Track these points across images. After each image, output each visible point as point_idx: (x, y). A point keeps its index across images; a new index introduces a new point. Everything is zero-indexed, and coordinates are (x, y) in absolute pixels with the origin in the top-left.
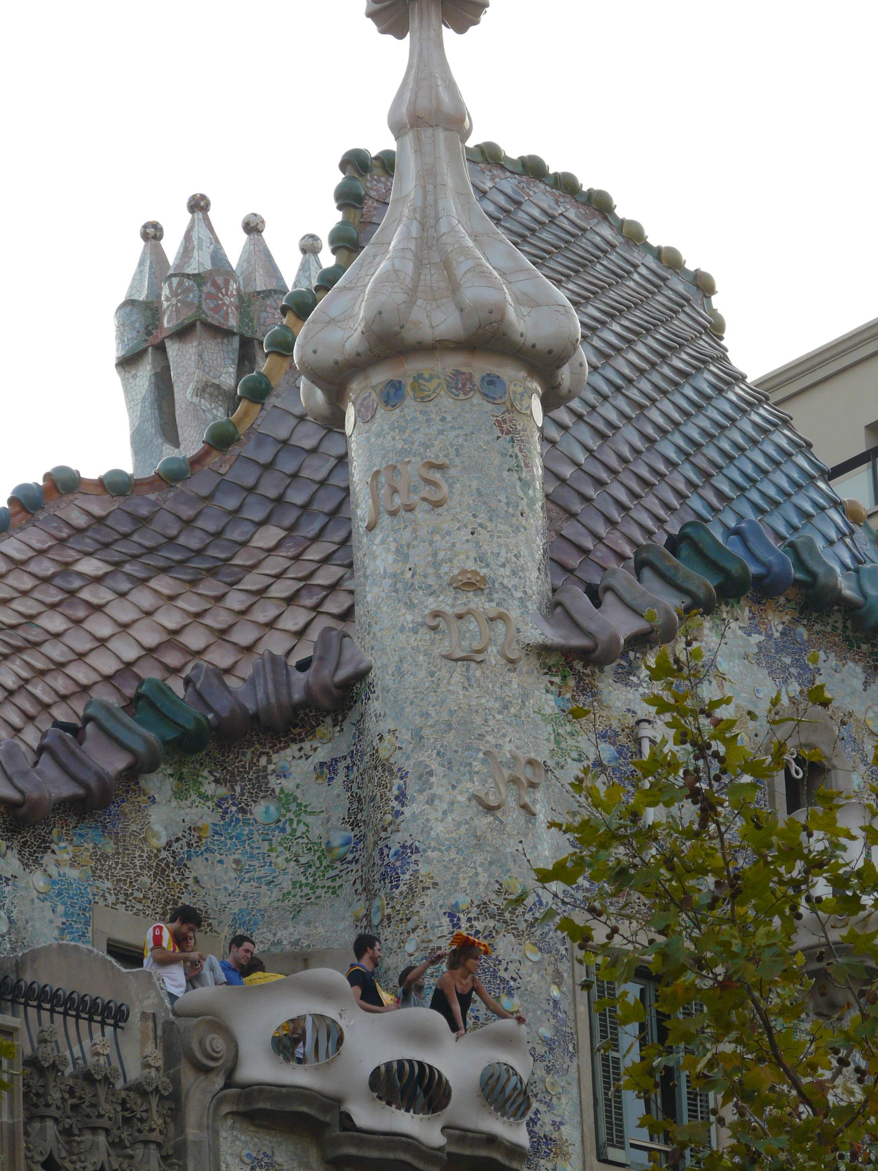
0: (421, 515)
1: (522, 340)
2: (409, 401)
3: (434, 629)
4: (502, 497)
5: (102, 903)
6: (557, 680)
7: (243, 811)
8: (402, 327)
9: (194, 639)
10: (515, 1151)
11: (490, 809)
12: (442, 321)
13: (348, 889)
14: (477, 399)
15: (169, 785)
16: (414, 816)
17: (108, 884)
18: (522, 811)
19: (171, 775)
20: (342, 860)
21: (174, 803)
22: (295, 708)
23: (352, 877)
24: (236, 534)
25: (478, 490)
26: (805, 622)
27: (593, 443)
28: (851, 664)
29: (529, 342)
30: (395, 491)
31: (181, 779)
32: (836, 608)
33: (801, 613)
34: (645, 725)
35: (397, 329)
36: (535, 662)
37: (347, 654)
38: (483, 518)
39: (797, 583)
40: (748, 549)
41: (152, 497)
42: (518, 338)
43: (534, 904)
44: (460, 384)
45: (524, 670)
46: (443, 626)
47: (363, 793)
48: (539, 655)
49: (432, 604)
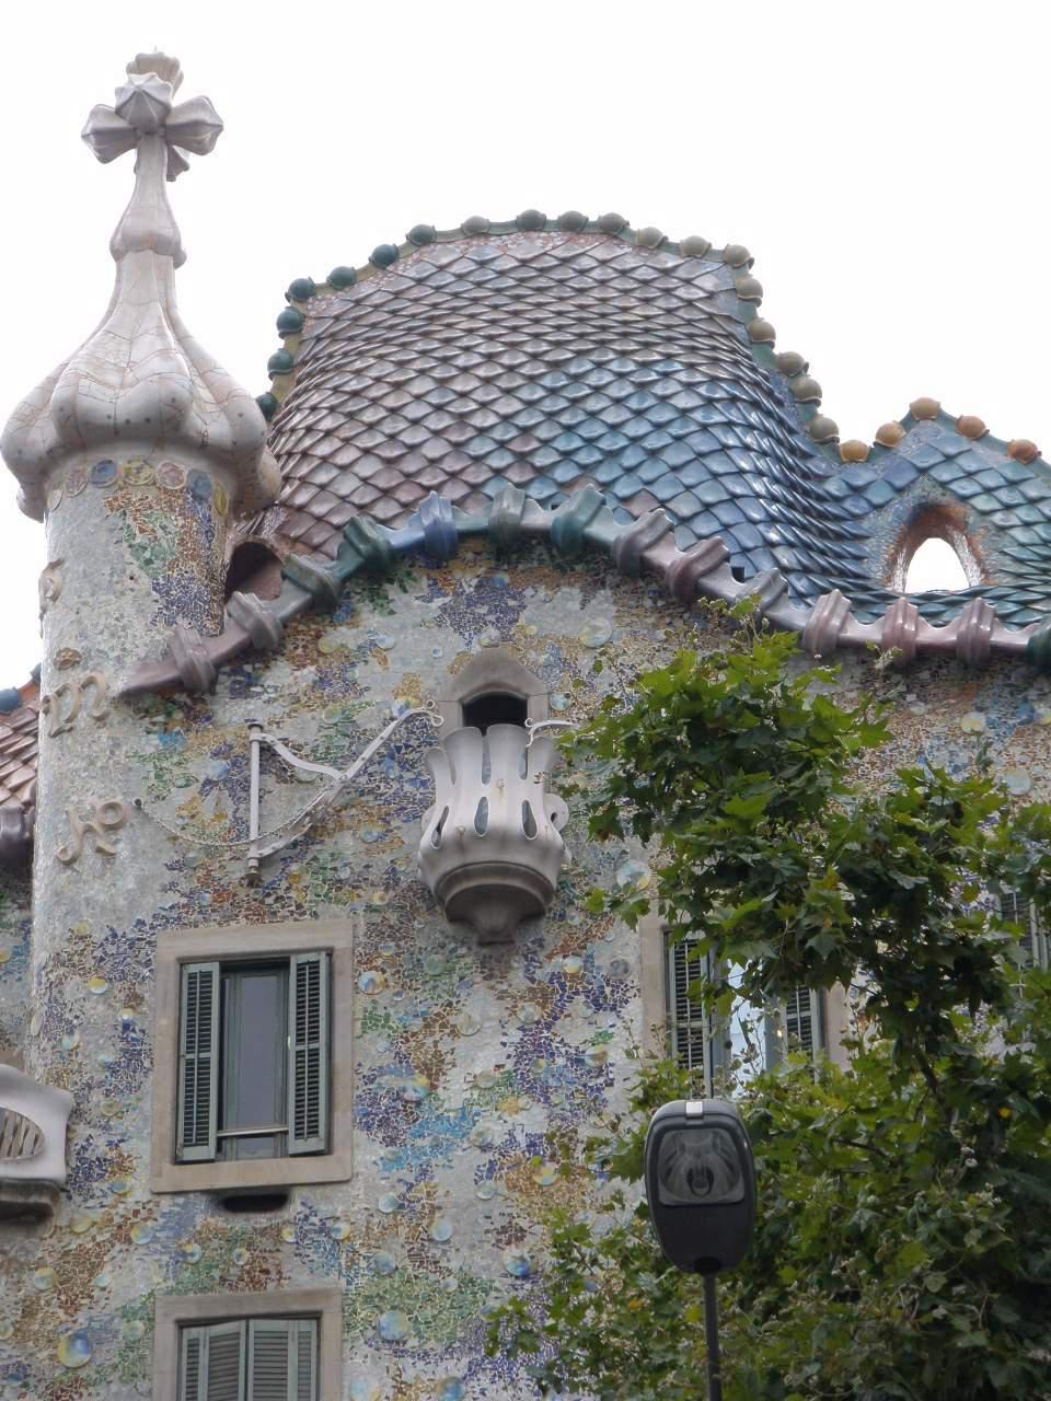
1: (112, 421)
6: (161, 718)
8: (20, 452)
11: (68, 864)
18: (99, 855)
25: (84, 571)
26: (506, 567)
28: (565, 589)
29: (121, 418)
32: (534, 542)
33: (498, 560)
34: (258, 729)
35: (17, 455)
38: (86, 595)
42: (107, 421)
43: (107, 939)
45: (115, 722)
48: (128, 704)
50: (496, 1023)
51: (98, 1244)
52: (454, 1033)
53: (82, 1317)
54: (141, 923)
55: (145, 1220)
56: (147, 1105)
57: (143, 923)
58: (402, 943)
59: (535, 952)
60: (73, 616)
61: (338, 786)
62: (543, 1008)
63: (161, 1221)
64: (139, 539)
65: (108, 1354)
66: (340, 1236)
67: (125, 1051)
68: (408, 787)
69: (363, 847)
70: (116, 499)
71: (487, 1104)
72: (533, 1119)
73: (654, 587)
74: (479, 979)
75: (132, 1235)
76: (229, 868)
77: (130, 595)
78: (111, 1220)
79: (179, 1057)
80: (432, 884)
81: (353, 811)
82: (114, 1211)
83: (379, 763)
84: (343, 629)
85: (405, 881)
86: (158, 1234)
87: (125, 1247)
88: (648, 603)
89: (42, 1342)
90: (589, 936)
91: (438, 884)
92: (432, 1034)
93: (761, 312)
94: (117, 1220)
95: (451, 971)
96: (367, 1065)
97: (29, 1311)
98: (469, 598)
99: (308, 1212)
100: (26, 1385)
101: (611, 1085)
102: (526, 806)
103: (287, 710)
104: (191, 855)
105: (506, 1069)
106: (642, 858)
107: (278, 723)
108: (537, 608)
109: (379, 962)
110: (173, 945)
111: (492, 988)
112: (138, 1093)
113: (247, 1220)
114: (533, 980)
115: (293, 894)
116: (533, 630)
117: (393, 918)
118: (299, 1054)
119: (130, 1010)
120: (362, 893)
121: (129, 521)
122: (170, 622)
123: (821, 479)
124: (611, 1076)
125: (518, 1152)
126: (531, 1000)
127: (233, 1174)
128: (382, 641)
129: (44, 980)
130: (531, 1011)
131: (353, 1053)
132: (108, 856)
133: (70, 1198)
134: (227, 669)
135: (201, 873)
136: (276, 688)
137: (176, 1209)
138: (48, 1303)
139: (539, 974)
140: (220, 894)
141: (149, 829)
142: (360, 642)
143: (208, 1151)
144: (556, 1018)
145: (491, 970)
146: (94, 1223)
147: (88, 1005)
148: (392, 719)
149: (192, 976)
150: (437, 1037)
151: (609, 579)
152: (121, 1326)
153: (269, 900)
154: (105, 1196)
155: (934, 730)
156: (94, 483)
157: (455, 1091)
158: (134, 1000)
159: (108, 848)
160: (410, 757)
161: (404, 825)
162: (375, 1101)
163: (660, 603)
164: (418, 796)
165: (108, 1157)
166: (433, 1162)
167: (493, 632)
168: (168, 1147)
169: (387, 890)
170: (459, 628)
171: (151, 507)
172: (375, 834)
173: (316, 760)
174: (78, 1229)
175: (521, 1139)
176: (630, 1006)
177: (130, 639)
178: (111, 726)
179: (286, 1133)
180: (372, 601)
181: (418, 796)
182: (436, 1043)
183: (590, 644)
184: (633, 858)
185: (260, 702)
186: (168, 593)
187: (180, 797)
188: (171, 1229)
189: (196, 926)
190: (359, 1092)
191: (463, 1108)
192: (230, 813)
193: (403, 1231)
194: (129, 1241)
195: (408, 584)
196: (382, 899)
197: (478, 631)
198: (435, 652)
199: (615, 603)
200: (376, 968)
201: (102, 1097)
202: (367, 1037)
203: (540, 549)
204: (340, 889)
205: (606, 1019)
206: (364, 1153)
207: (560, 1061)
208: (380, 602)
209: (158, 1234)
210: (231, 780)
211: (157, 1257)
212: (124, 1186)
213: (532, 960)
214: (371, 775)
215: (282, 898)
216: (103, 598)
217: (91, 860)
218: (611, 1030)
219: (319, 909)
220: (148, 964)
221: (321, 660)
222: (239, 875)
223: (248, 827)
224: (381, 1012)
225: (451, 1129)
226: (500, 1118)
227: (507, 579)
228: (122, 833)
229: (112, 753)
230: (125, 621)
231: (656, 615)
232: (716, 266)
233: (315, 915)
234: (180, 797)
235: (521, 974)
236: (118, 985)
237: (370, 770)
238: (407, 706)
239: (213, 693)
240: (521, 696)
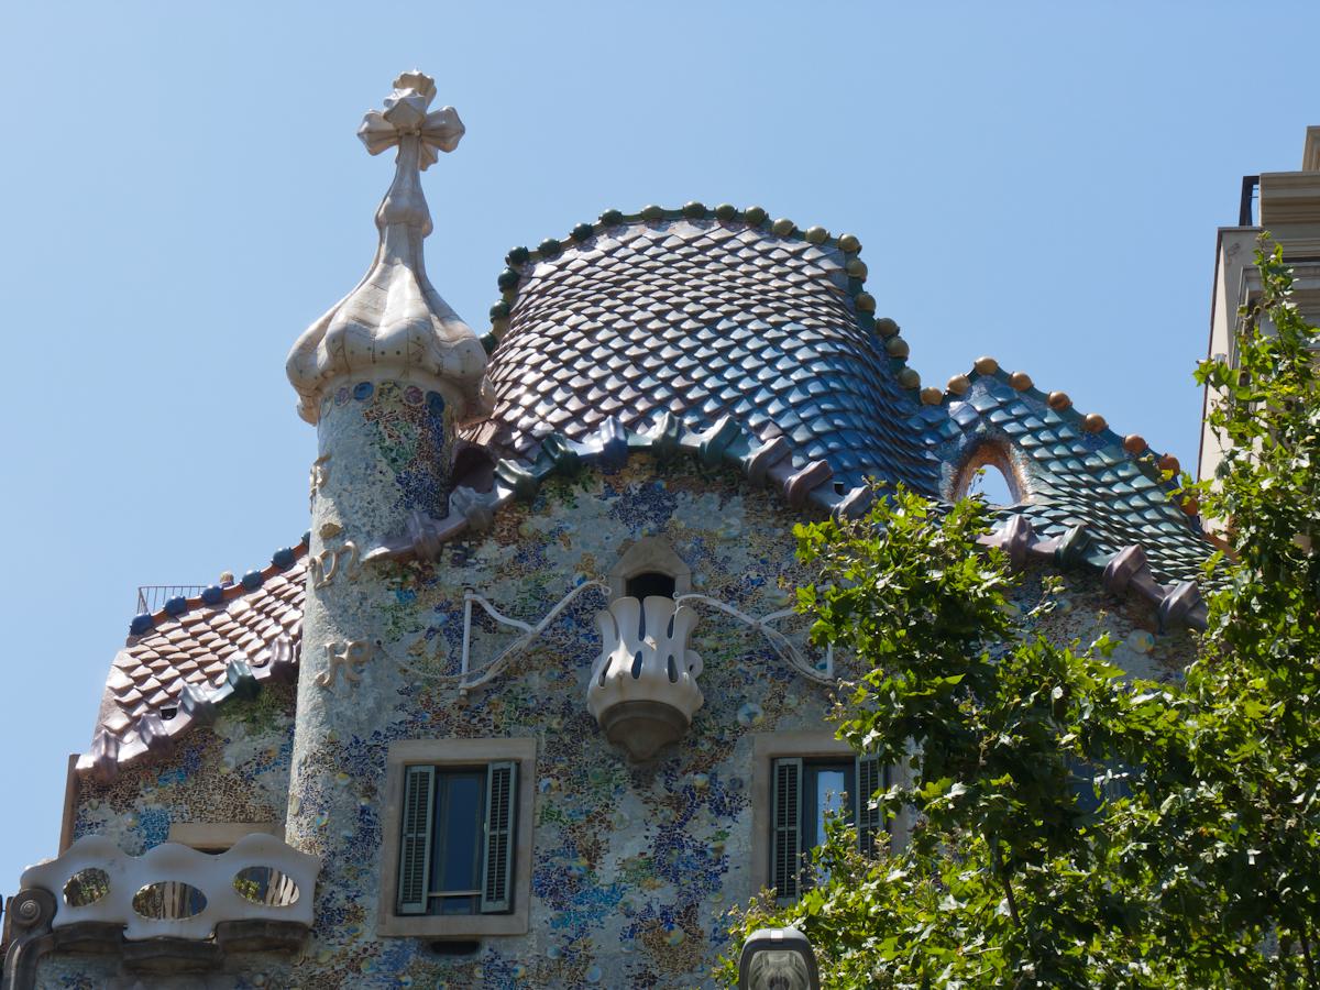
6: (399, 580)
19: (245, 721)
21: (247, 739)
28: (708, 495)
31: (254, 720)
32: (686, 458)
33: (658, 470)
50: (640, 821)
51: (336, 972)
52: (609, 828)
54: (377, 733)
55: (372, 956)
56: (376, 870)
57: (379, 734)
58: (573, 758)
59: (673, 769)
61: (530, 637)
62: (678, 811)
63: (384, 957)
64: (388, 442)
66: (519, 975)
67: (362, 829)
68: (582, 640)
70: (372, 412)
71: (632, 881)
72: (664, 894)
73: (774, 496)
74: (630, 788)
75: (362, 966)
76: (445, 695)
77: (379, 486)
78: (347, 954)
79: (401, 837)
80: (598, 715)
81: (541, 656)
82: (348, 948)
83: (562, 621)
84: (539, 517)
85: (577, 711)
86: (381, 967)
87: (356, 975)
88: (770, 508)
90: (714, 758)
91: (603, 714)
92: (593, 827)
93: (865, 287)
94: (351, 954)
95: (609, 781)
96: (544, 849)
98: (635, 498)
99: (493, 955)
101: (726, 871)
102: (671, 659)
103: (493, 577)
104: (417, 684)
105: (648, 856)
106: (757, 702)
107: (486, 587)
108: (686, 508)
109: (555, 771)
110: (403, 752)
111: (639, 794)
112: (370, 862)
113: (448, 959)
114: (670, 791)
115: (492, 717)
116: (682, 525)
117: (567, 739)
118: (492, 838)
119: (366, 799)
120: (545, 719)
121: (381, 428)
122: (409, 507)
123: (909, 416)
124: (726, 864)
125: (655, 920)
126: (669, 805)
127: (438, 926)
128: (568, 528)
129: (303, 772)
131: (533, 839)
132: (355, 684)
133: (316, 937)
134: (450, 544)
135: (424, 698)
136: (486, 560)
137: (396, 949)
139: (675, 786)
140: (439, 713)
141: (385, 662)
142: (552, 528)
143: (421, 907)
144: (687, 820)
145: (639, 781)
146: (334, 956)
147: (335, 793)
148: (573, 588)
149: (414, 775)
150: (596, 830)
151: (741, 489)
153: (475, 721)
154: (343, 936)
156: (356, 398)
157: (608, 871)
158: (370, 791)
159: (356, 677)
160: (584, 617)
161: (578, 669)
162: (547, 875)
163: (779, 509)
164: (590, 647)
165: (346, 907)
166: (590, 923)
167: (652, 525)
168: (390, 902)
169: (563, 718)
170: (626, 520)
171: (398, 419)
172: (556, 674)
173: (514, 616)
174: (322, 960)
175: (656, 908)
176: (743, 813)
177: (378, 519)
178: (361, 583)
179: (480, 896)
180: (561, 497)
181: (590, 647)
182: (595, 834)
183: (725, 536)
184: (751, 701)
185: (473, 571)
186: (407, 484)
187: (411, 640)
188: (391, 963)
189: (419, 738)
190: (536, 868)
191: (614, 884)
192: (448, 654)
193: (565, 973)
196: (559, 723)
197: (640, 524)
198: (607, 538)
199: (745, 507)
200: (552, 776)
201: (343, 862)
202: (543, 827)
203: (691, 464)
204: (527, 715)
205: (725, 822)
206: (538, 913)
207: (688, 852)
208: (567, 498)
209: (381, 967)
210: (449, 629)
211: (380, 984)
212: (357, 930)
213: (671, 775)
214: (554, 630)
215: (484, 719)
216: (359, 486)
218: (727, 831)
220: (381, 764)
221: (521, 540)
222: (452, 701)
224: (556, 809)
226: (641, 892)
228: (365, 666)
229: (361, 604)
230: (374, 504)
231: (777, 517)
232: (833, 250)
233: (509, 734)
234: (411, 640)
235: (662, 785)
236: (359, 779)
237: (554, 626)
238: (584, 578)
239: (439, 562)
240: (671, 575)
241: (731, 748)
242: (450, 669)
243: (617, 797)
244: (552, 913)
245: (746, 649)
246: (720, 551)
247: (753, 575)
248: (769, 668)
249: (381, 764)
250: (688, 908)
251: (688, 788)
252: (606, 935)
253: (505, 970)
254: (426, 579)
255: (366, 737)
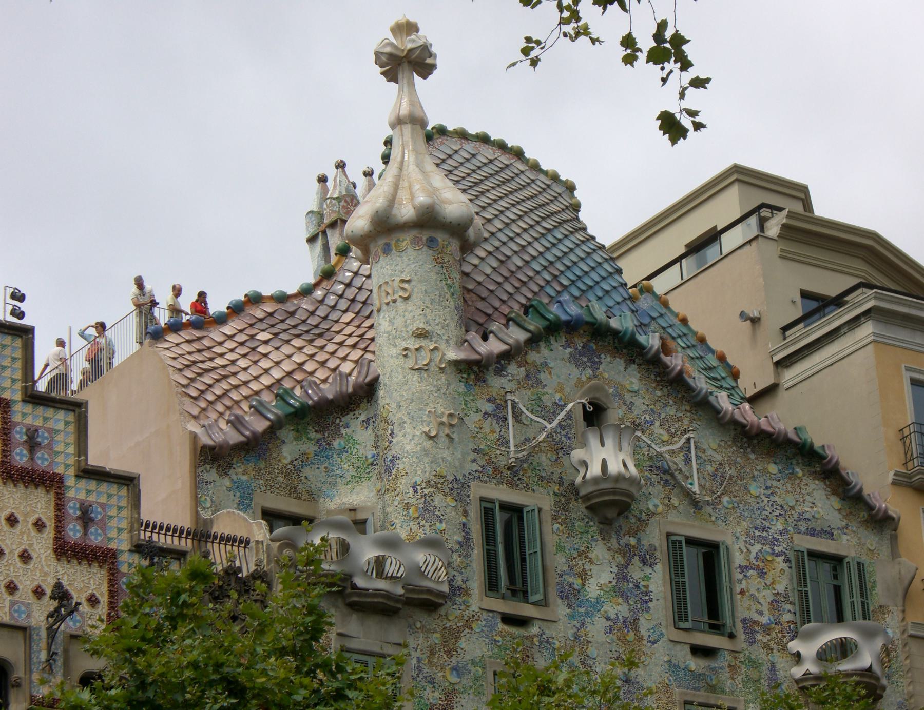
0: (400, 303)
2: (394, 252)
3: (406, 356)
4: (437, 293)
5: (259, 491)
6: (465, 376)
7: (329, 444)
9: (309, 367)
10: (441, 595)
11: (431, 438)
12: (406, 212)
13: (374, 477)
14: (425, 249)
15: (292, 435)
16: (398, 443)
17: (262, 482)
20: (372, 464)
22: (350, 396)
23: (376, 472)
24: (334, 316)
27: (495, 264)
29: (448, 220)
30: (388, 294)
31: (298, 431)
36: (454, 369)
37: (371, 370)
39: (587, 323)
40: (564, 310)
41: (295, 302)
44: (415, 241)
46: (409, 354)
47: (379, 433)
48: (455, 365)
49: (404, 345)
52: (591, 561)
53: (454, 660)
54: (464, 475)
60: (420, 312)
63: (484, 622)
65: (467, 680)
68: (563, 438)
69: (550, 463)
73: (657, 370)
75: (474, 626)
81: (545, 444)
88: (653, 377)
89: (439, 668)
94: (466, 618)
95: (587, 532)
97: (432, 653)
100: (434, 687)
104: (482, 447)
109: (560, 520)
110: (478, 490)
116: (606, 375)
117: (563, 500)
129: (419, 491)
130: (620, 559)
135: (487, 457)
138: (440, 650)
140: (496, 470)
147: (448, 510)
151: (637, 360)
152: (473, 669)
153: (516, 479)
155: (758, 468)
157: (592, 590)
158: (465, 513)
163: (658, 379)
193: (577, 649)
194: (471, 629)
195: (558, 338)
197: (584, 369)
203: (610, 338)
205: (648, 570)
206: (561, 610)
217: (443, 440)
219: (535, 488)
222: (503, 463)
223: (508, 442)
225: (593, 606)
227: (595, 347)
233: (533, 490)
239: (488, 370)
241: (647, 524)
242: (500, 443)
243: (594, 544)
244: (568, 611)
245: (648, 463)
246: (627, 396)
247: (648, 418)
248: (661, 478)
249: (468, 496)
250: (634, 620)
251: (627, 545)
252: (597, 628)
253: (548, 642)
254: (480, 379)
255: (460, 477)
